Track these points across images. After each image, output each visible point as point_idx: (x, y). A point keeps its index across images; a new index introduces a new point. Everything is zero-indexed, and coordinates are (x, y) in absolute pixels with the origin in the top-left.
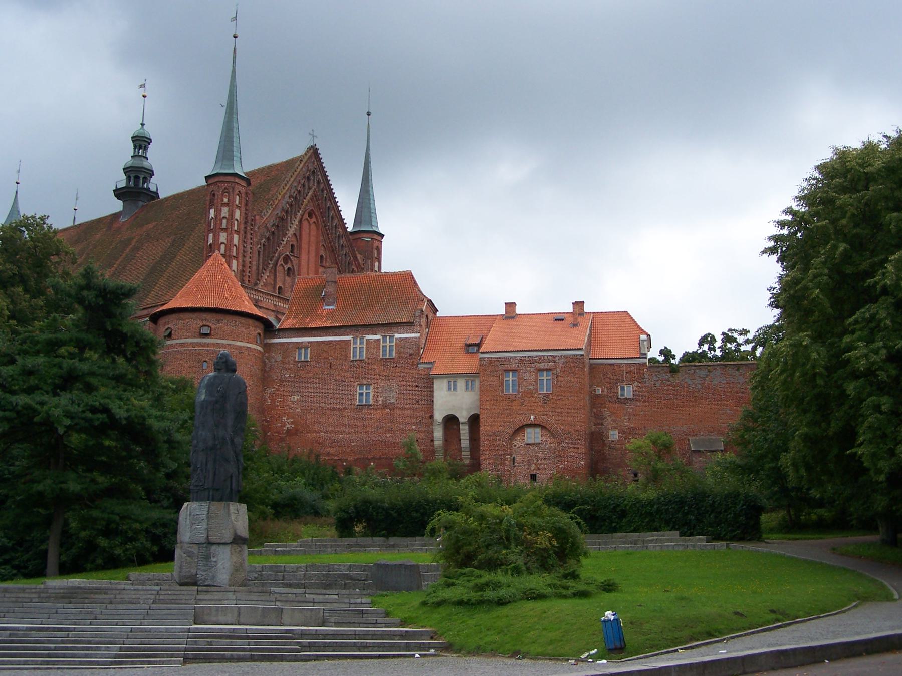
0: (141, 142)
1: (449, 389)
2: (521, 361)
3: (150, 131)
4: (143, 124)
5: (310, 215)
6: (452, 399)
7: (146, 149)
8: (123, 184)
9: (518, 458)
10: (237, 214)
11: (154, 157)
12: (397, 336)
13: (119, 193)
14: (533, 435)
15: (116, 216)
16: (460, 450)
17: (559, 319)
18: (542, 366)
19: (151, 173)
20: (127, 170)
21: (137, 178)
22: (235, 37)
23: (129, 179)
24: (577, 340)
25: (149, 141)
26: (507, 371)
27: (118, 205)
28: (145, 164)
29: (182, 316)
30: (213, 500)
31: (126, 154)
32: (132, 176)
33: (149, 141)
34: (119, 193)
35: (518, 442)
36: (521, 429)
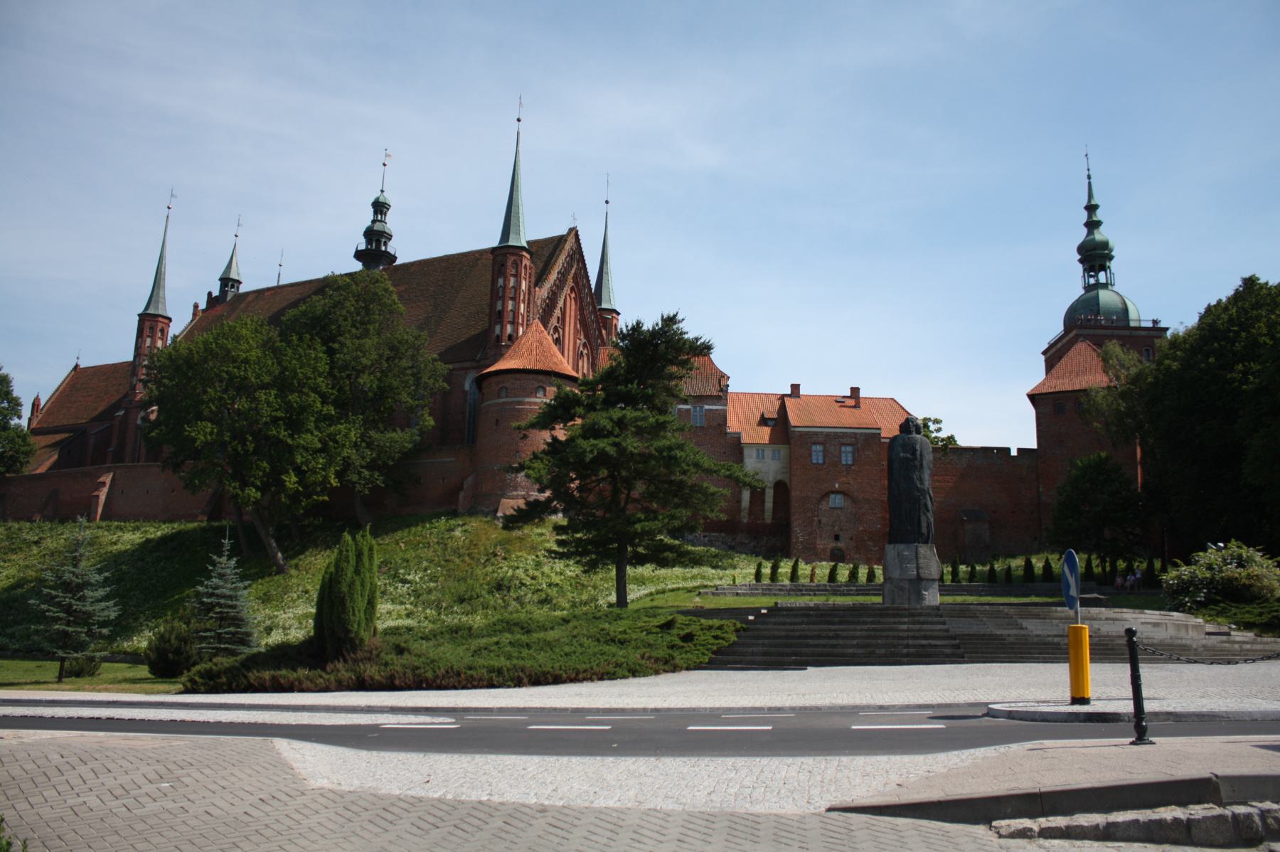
0: (380, 207)
1: (758, 457)
2: (828, 435)
3: (389, 197)
5: (572, 289)
6: (763, 465)
8: (362, 247)
9: (824, 520)
10: (524, 286)
11: (392, 222)
12: (707, 407)
13: (359, 255)
14: (837, 501)
16: (763, 511)
17: (840, 401)
18: (844, 441)
19: (389, 237)
21: (378, 242)
22: (519, 120)
24: (848, 419)
26: (815, 443)
27: (357, 266)
29: (518, 376)
31: (367, 216)
34: (359, 255)
35: (823, 506)
36: (827, 495)
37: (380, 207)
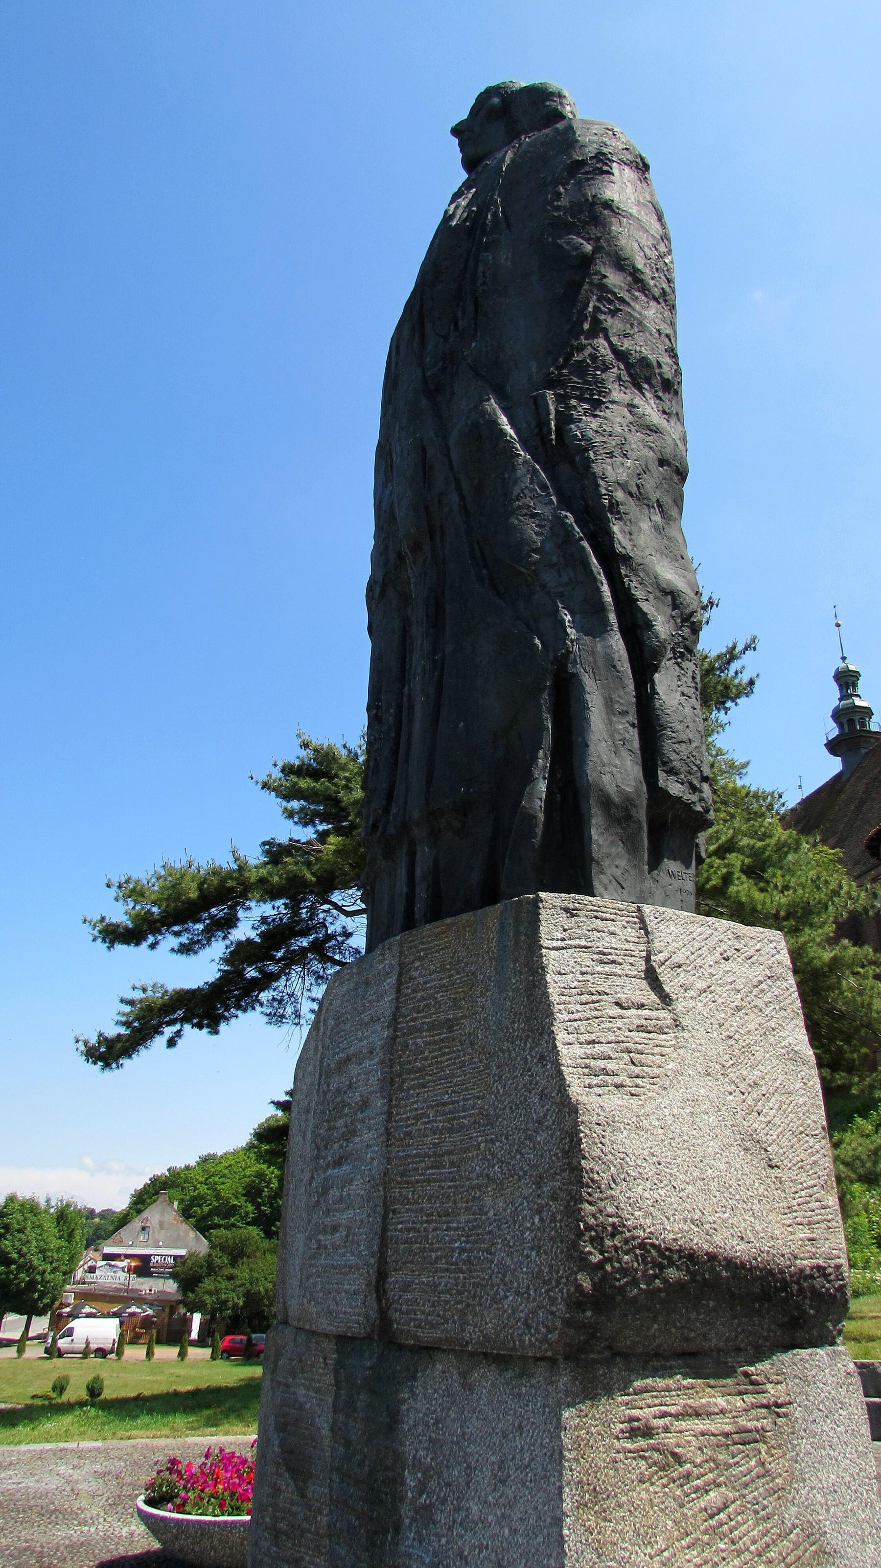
0: (846, 680)
4: (844, 659)
7: (855, 685)
13: (833, 747)
15: (837, 778)
20: (837, 715)
21: (851, 722)
23: (840, 725)
25: (856, 675)
27: (834, 765)
28: (858, 702)
30: (435, 914)
31: (832, 696)
32: (844, 721)
33: (856, 675)
34: (833, 747)
37: (846, 680)
